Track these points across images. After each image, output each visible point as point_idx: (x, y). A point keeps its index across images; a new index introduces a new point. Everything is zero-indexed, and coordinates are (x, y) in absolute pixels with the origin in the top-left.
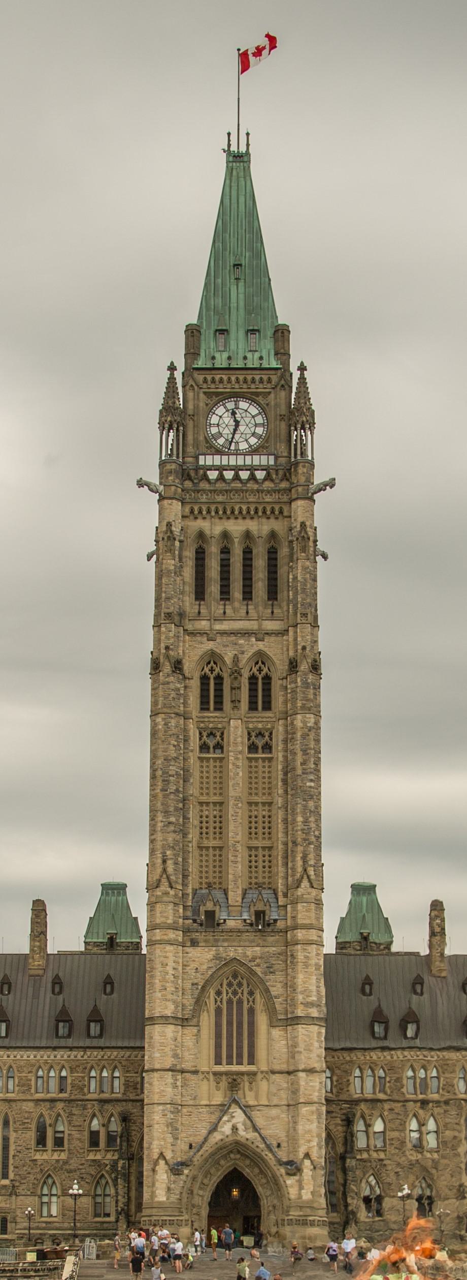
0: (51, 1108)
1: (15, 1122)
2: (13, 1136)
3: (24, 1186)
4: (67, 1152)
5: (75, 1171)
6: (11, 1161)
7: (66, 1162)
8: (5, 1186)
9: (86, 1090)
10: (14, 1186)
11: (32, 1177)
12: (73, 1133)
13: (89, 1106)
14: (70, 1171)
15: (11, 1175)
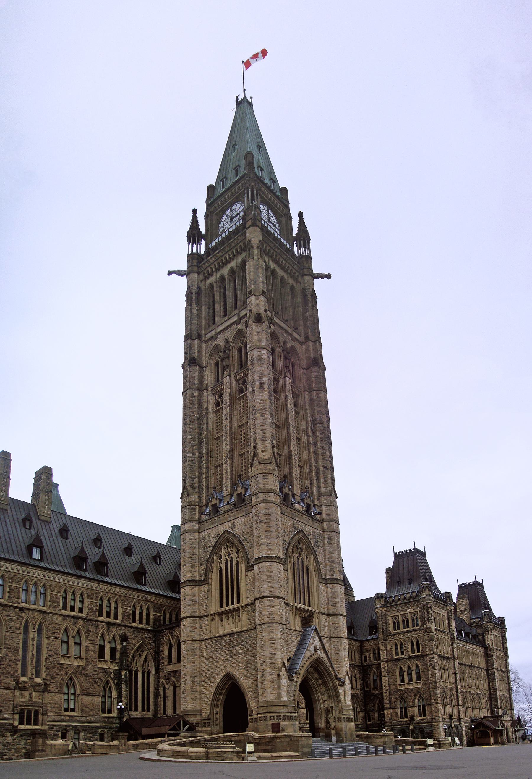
0: (74, 624)
1: (47, 631)
2: (45, 642)
3: (53, 685)
4: (84, 660)
5: (90, 676)
6: (44, 663)
7: (84, 668)
8: (38, 684)
9: (97, 613)
10: (46, 684)
11: (59, 678)
12: (89, 645)
13: (100, 626)
14: (87, 676)
15: (44, 675)
